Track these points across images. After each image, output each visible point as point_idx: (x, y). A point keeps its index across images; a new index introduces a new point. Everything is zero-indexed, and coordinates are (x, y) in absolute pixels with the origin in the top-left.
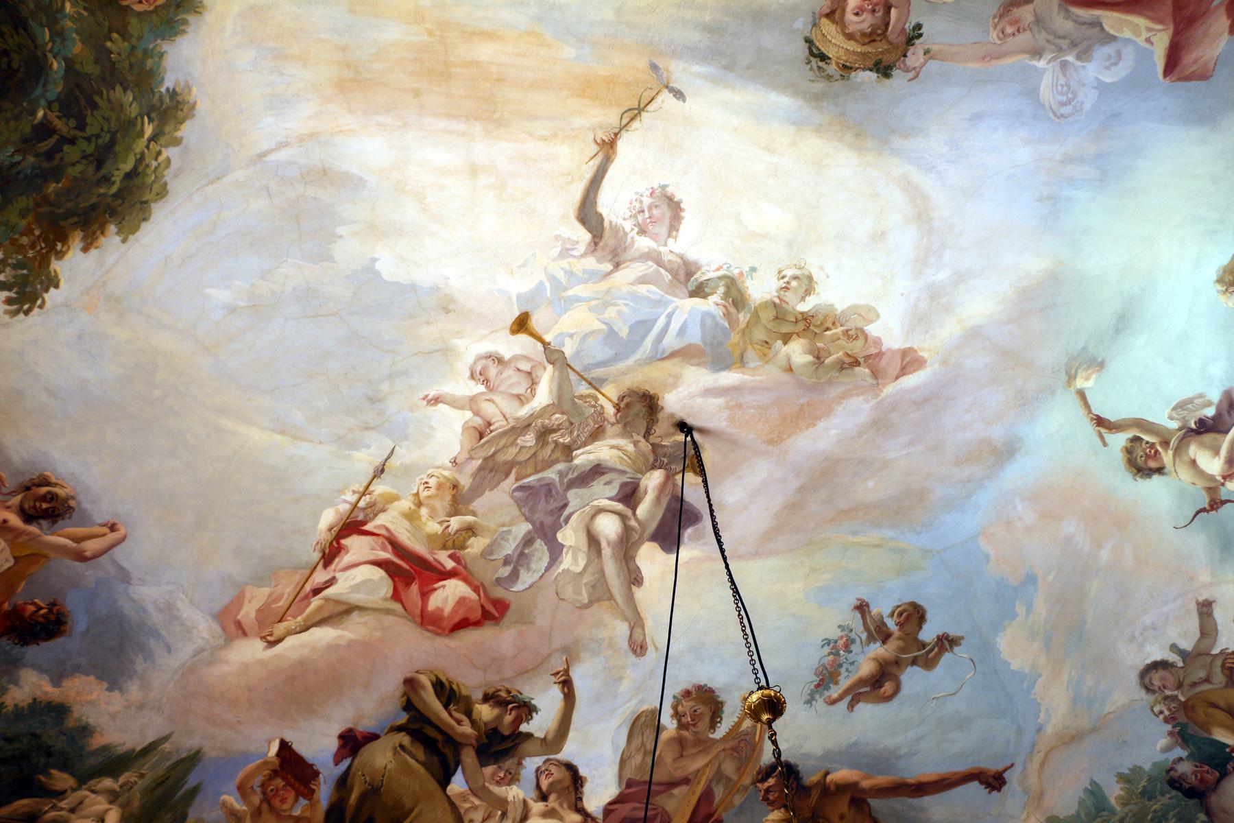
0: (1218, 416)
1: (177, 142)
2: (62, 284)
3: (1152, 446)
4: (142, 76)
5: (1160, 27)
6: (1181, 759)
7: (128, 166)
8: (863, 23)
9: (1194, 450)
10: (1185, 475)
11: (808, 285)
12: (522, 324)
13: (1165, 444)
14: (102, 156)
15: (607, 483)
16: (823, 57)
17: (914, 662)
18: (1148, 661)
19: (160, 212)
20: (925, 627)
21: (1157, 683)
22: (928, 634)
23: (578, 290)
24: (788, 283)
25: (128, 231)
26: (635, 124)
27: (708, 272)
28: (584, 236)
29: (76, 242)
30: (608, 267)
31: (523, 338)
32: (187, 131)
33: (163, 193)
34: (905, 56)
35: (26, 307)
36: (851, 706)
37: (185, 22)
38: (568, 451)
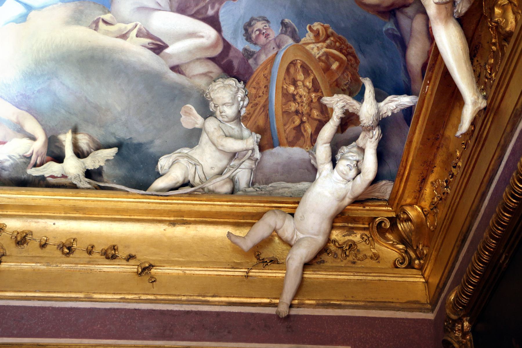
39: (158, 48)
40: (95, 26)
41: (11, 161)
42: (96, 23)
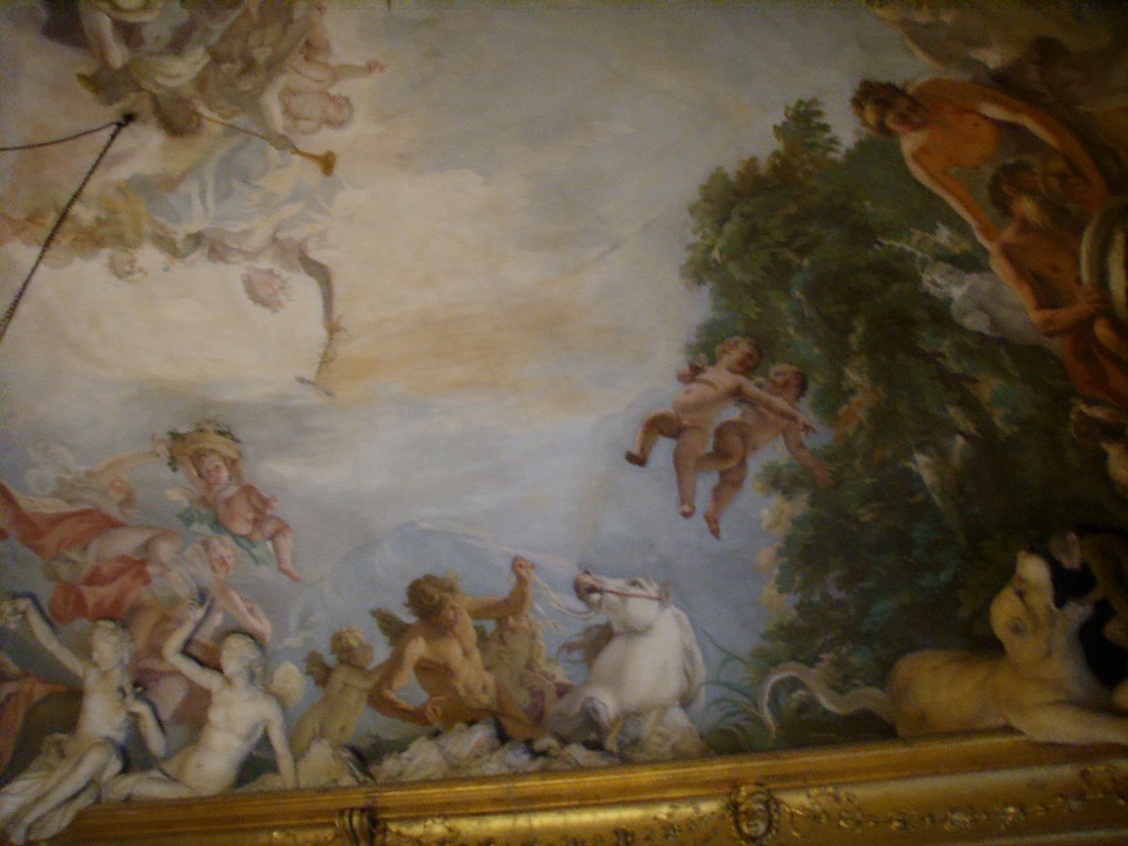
1: (691, 247)
2: (771, 129)
4: (727, 291)
7: (729, 228)
8: (211, 462)
11: (114, 268)
12: (327, 163)
14: (752, 236)
15: (158, 38)
19: (694, 196)
23: (294, 209)
24: (132, 267)
25: (718, 177)
26: (321, 351)
27: (199, 256)
28: (315, 254)
29: (763, 167)
30: (282, 236)
31: (319, 151)
32: (683, 256)
33: (693, 210)
35: (802, 109)
37: (698, 336)
38: (217, 58)
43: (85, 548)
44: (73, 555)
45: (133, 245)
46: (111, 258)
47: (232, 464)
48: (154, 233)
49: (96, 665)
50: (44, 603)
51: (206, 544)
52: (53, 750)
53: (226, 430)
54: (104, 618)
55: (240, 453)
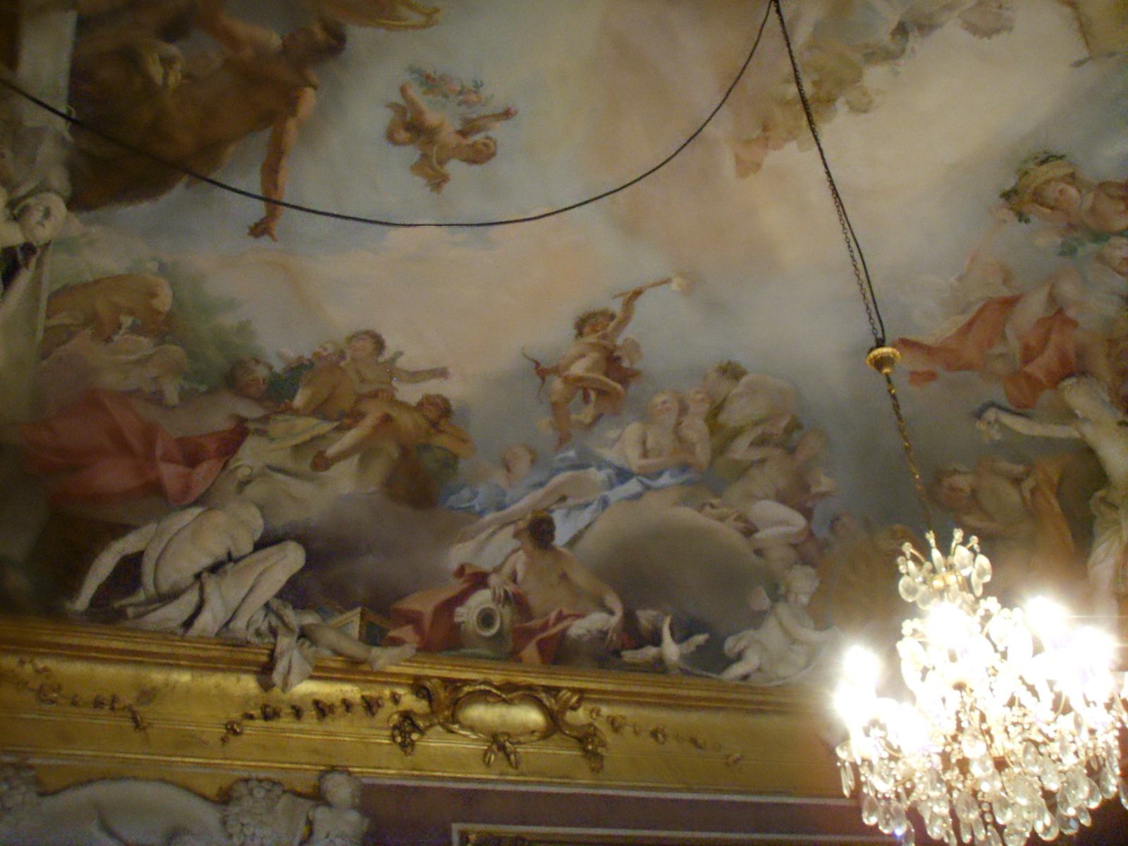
0: (620, 369)
3: (604, 328)
5: (938, 342)
6: (271, 368)
8: (1051, 193)
9: (594, 355)
10: (573, 351)
11: (855, 109)
13: (604, 337)
16: (1043, 162)
17: (424, 156)
18: (384, 337)
20: (464, 165)
21: (359, 344)
22: (455, 168)
27: (914, 41)
34: (1011, 209)
36: (394, 106)
39: (749, 531)
40: (700, 509)
41: (590, 636)
42: (703, 505)
43: (1004, 337)
44: (999, 349)
45: (859, 76)
46: (848, 103)
47: (1072, 178)
48: (865, 55)
49: (1085, 420)
50: (1004, 401)
51: (1101, 258)
52: (1102, 507)
53: (1045, 156)
54: (1063, 379)
55: (1071, 164)
